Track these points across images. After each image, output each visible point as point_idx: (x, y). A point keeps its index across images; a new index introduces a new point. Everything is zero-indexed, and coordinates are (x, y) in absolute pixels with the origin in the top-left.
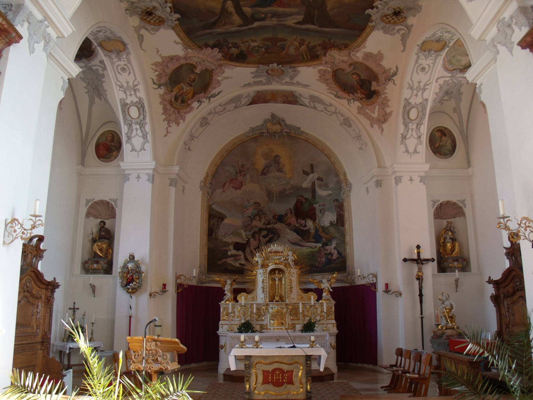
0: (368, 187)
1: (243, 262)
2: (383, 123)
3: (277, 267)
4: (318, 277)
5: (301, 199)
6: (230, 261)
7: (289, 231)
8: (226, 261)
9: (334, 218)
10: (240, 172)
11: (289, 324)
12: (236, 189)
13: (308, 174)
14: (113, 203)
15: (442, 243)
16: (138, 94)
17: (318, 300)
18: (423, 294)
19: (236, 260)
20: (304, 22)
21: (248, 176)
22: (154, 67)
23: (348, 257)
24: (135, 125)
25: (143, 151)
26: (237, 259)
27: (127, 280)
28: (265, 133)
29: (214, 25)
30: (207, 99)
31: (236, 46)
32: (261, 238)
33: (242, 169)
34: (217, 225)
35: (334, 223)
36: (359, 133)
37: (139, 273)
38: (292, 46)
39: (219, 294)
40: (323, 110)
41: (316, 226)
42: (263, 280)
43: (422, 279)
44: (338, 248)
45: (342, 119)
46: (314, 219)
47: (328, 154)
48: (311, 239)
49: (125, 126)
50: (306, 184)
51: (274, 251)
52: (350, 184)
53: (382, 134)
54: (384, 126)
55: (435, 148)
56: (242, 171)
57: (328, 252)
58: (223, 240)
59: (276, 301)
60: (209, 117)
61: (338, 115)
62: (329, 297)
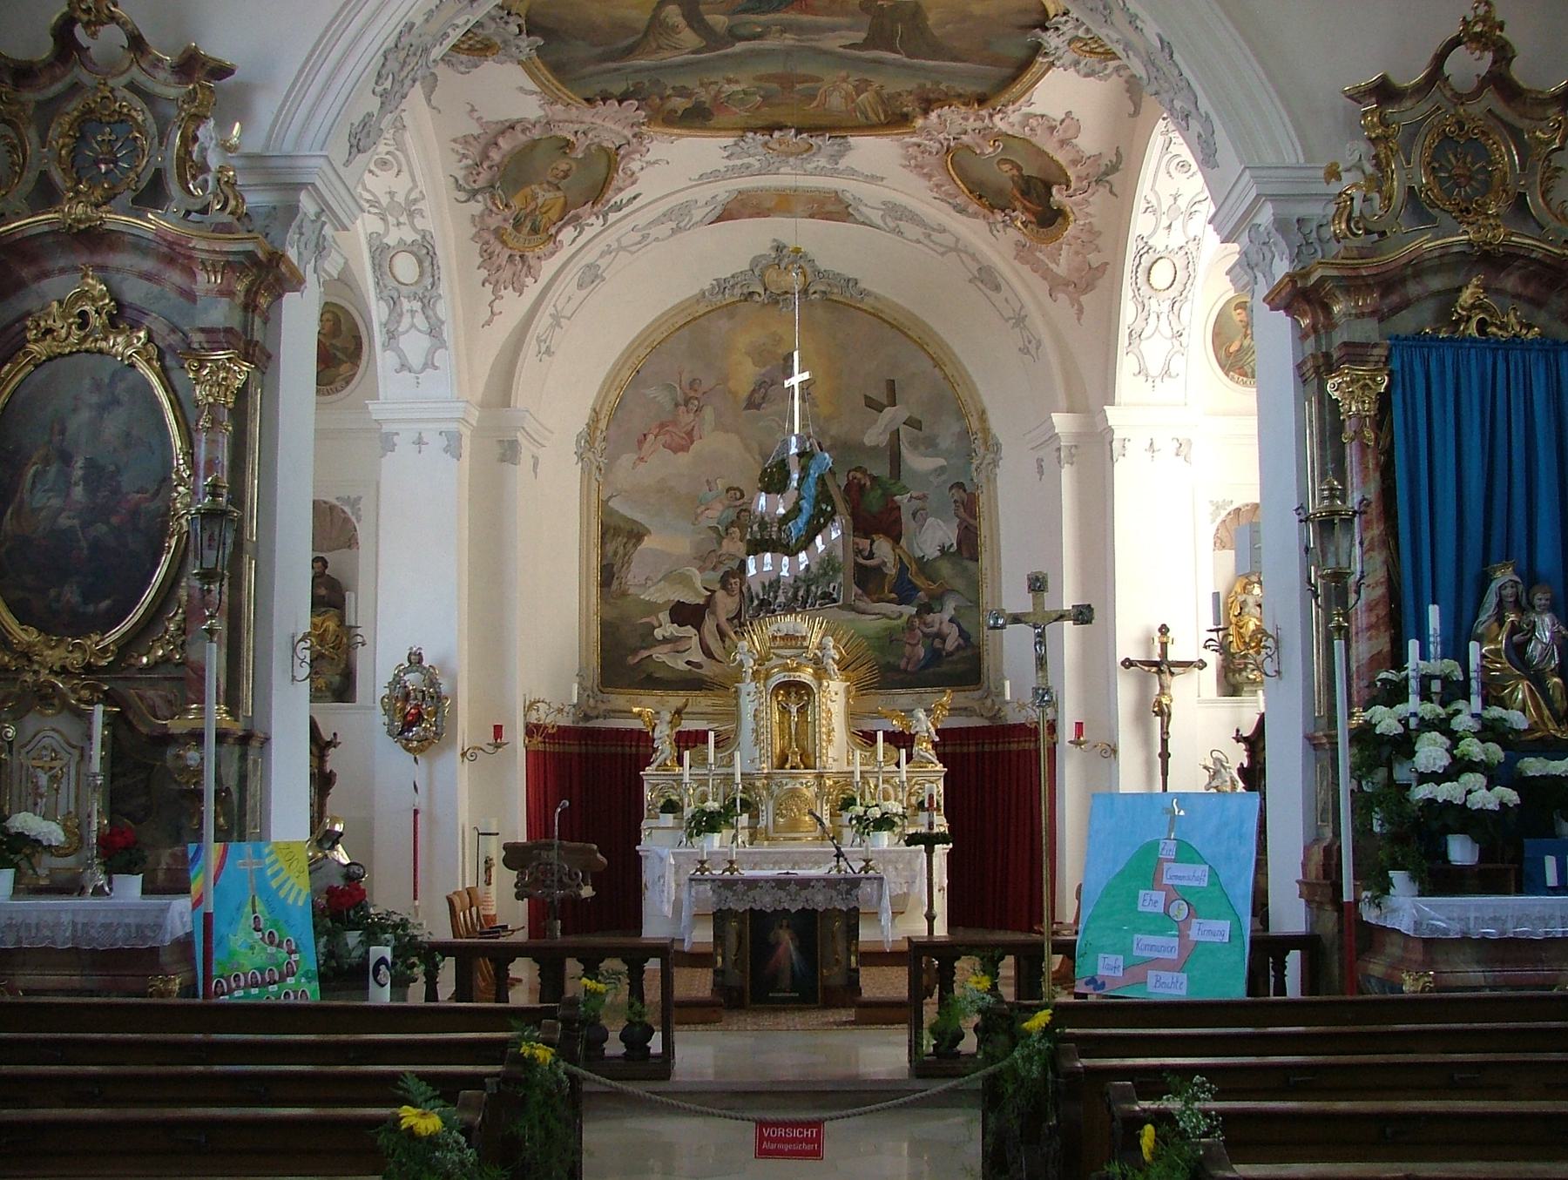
0: (1042, 460)
1: (698, 656)
2: (1085, 291)
4: (904, 698)
5: (860, 480)
6: (660, 654)
9: (951, 535)
10: (687, 402)
12: (675, 451)
13: (880, 408)
14: (346, 509)
15: (1236, 616)
16: (419, 223)
18: (1169, 751)
19: (678, 652)
20: (866, 45)
21: (708, 413)
22: (458, 147)
24: (409, 301)
25: (430, 371)
27: (405, 717)
28: (760, 295)
29: (629, 51)
30: (598, 218)
31: (682, 92)
33: (692, 394)
34: (625, 555)
35: (952, 550)
36: (1021, 309)
37: (438, 698)
38: (836, 93)
39: (637, 747)
40: (922, 238)
41: (900, 558)
42: (756, 710)
43: (1169, 715)
45: (974, 267)
46: (896, 539)
47: (938, 359)
49: (382, 303)
50: (875, 436)
52: (998, 446)
53: (1079, 319)
54: (1083, 299)
55: (1228, 355)
56: (690, 399)
57: (935, 629)
59: (792, 768)
60: (603, 263)
61: (962, 255)
62: (931, 754)
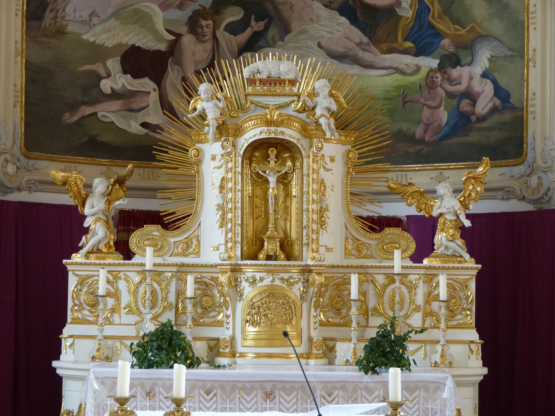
3: (273, 136)
7: (324, 12)
8: (96, 114)
11: (310, 340)
17: (417, 258)
23: (534, 106)
26: (135, 106)
32: (221, 34)
42: (223, 179)
44: (496, 75)
48: (400, 40)
51: (264, 76)
57: (462, 88)
58: (85, 37)
59: (269, 258)
